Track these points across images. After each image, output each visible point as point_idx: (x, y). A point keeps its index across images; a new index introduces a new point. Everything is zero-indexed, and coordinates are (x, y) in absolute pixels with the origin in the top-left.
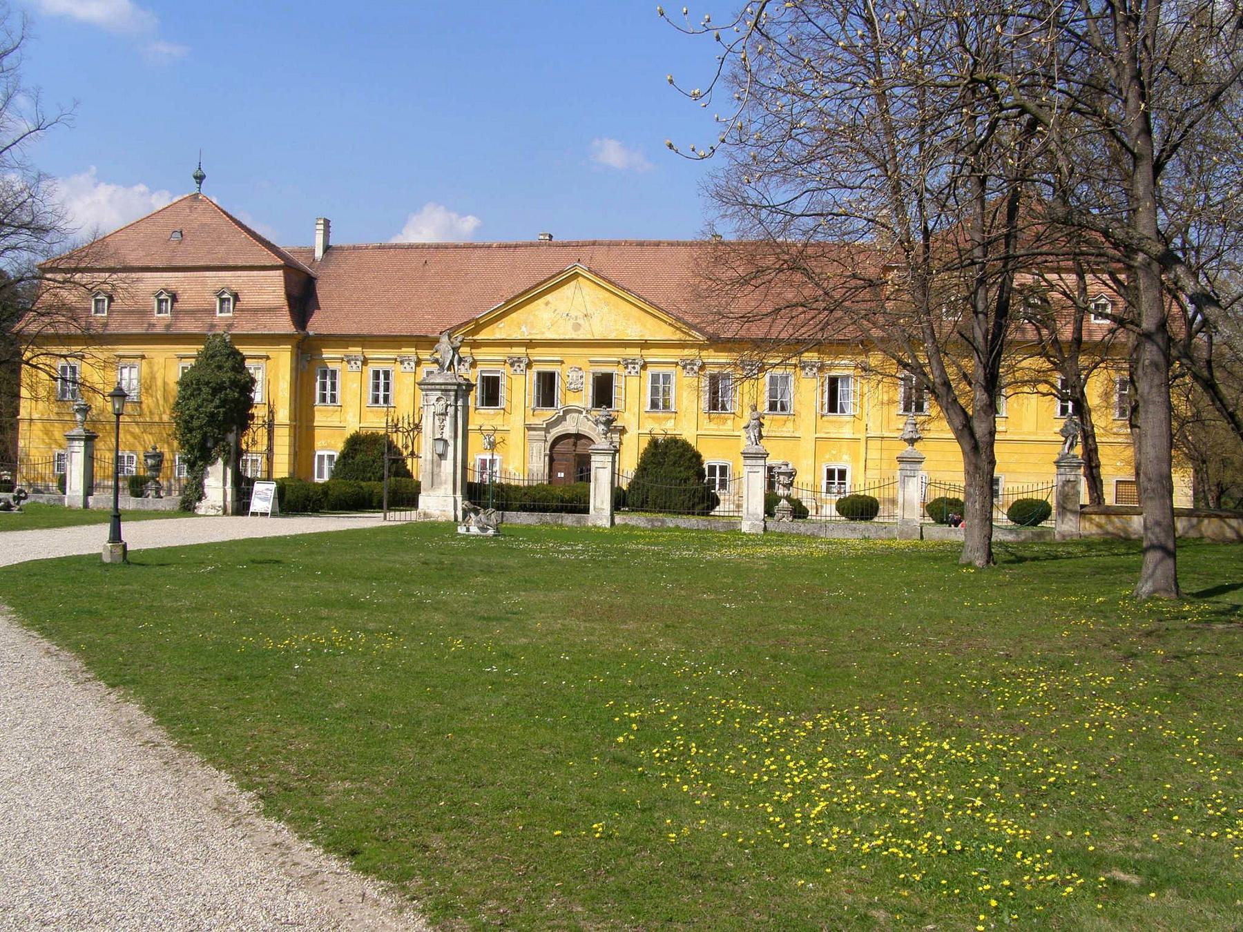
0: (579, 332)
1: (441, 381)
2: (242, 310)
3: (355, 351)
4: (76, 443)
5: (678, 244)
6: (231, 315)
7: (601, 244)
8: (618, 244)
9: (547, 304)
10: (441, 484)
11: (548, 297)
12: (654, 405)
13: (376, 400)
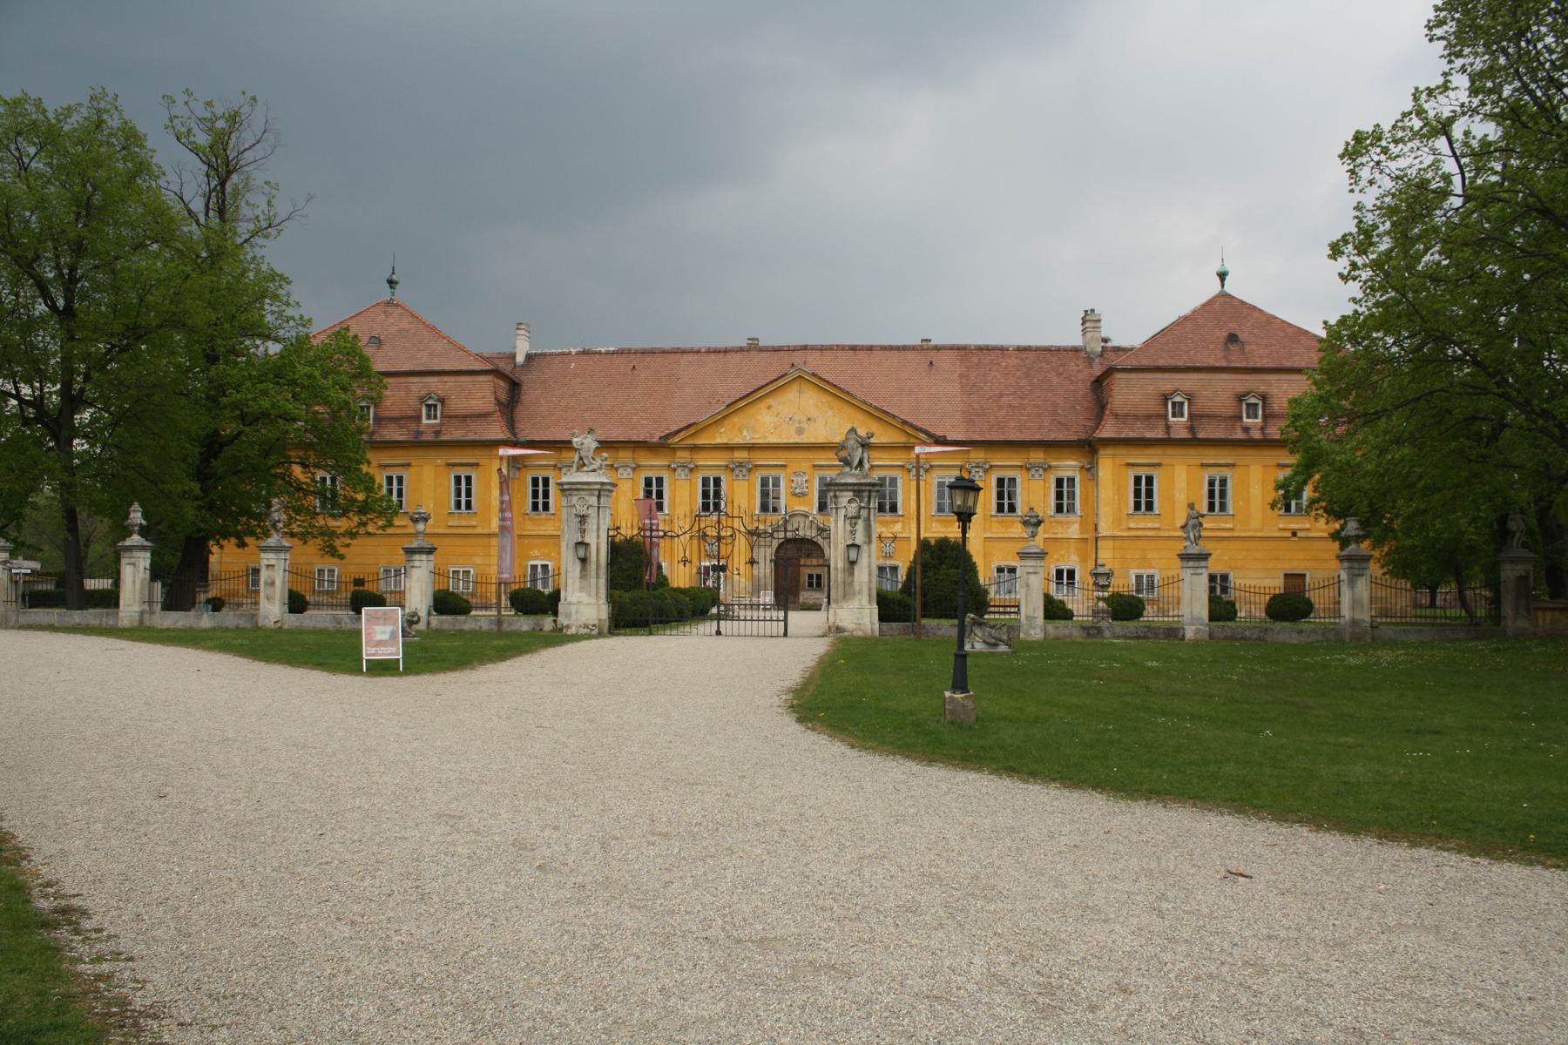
2: (450, 417)
4: (417, 557)
6: (438, 421)
9: (769, 407)
10: (854, 594)
11: (771, 401)
12: (1000, 508)
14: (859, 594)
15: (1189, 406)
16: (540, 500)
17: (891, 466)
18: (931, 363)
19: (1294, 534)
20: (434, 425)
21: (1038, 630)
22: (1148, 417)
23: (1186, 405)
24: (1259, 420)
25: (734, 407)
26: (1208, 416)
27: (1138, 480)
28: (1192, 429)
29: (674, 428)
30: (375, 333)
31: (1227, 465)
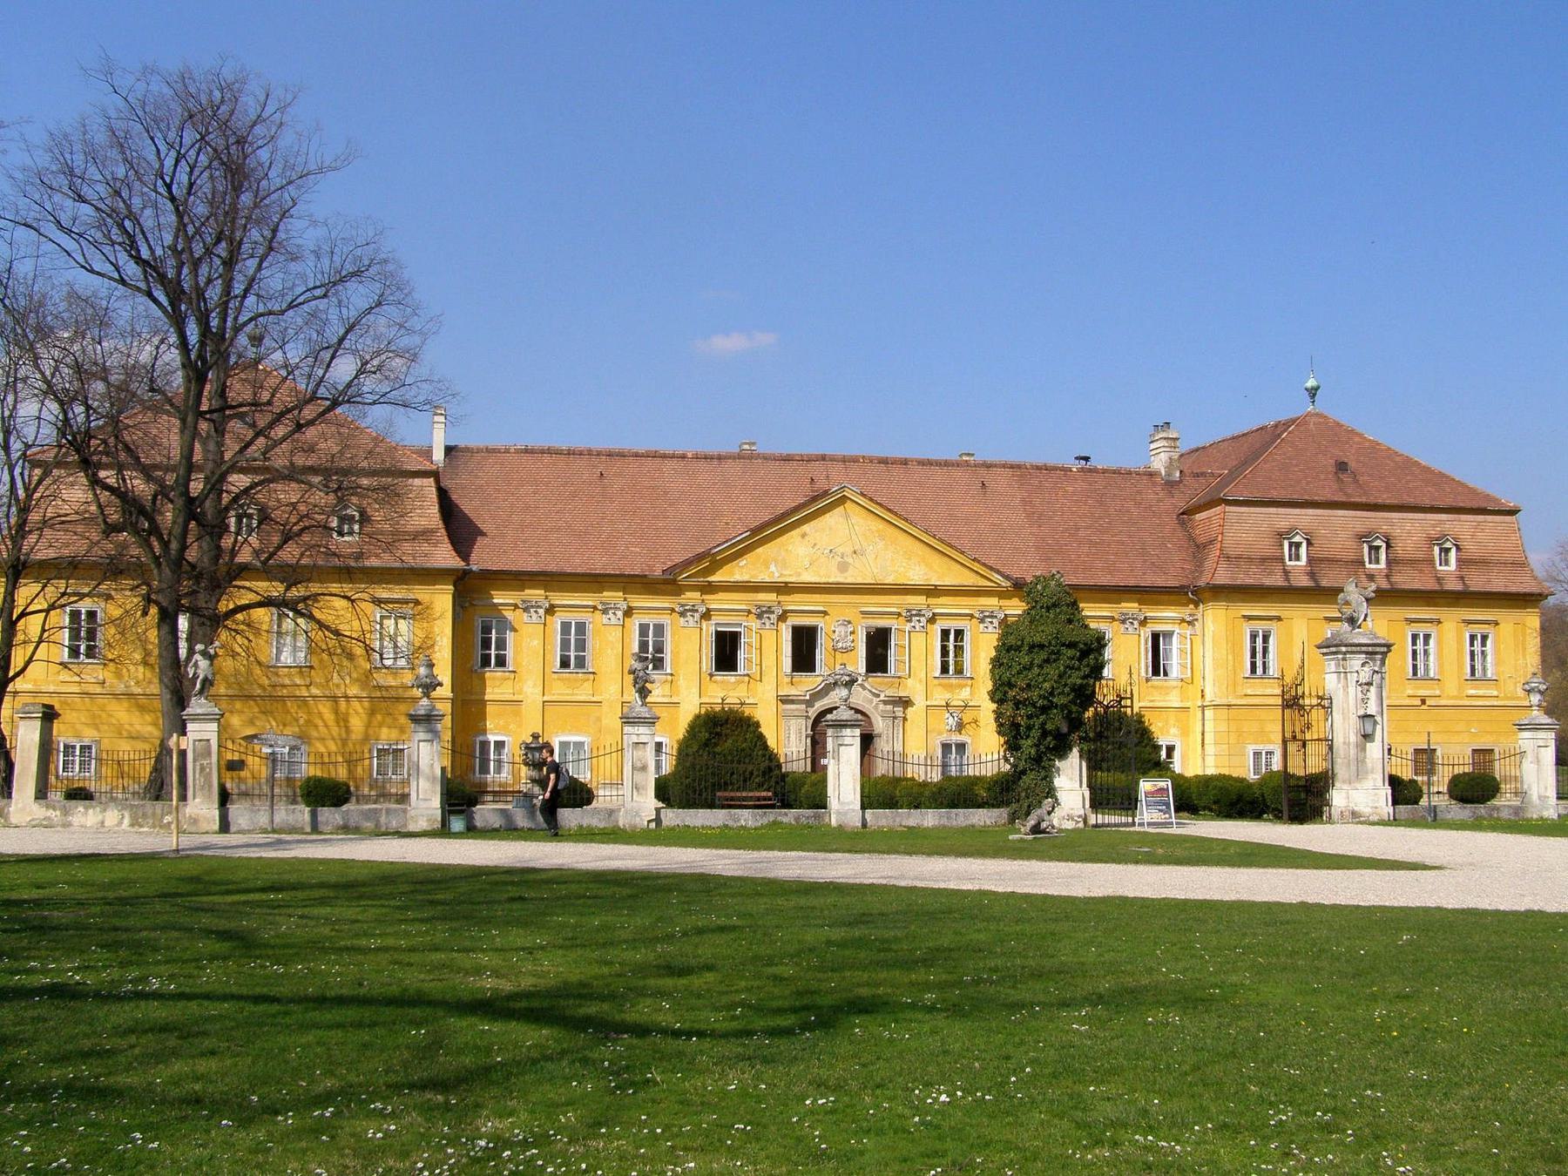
0: (845, 574)
3: (535, 594)
4: (848, 732)
5: (930, 463)
7: (833, 459)
8: (855, 460)
9: (804, 536)
11: (806, 528)
13: (945, 669)
14: (1372, 772)
15: (1387, 549)
17: (956, 615)
19: (1423, 702)
21: (1552, 810)
22: (1263, 560)
23: (1304, 545)
24: (1383, 565)
26: (1328, 560)
28: (1312, 575)
31: (1430, 621)
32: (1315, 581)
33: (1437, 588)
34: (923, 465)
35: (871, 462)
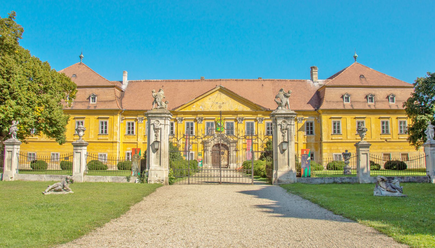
0: (221, 109)
1: (284, 112)
6: (96, 103)
9: (210, 99)
16: (131, 130)
18: (263, 85)
20: (94, 104)
22: (337, 102)
25: (198, 98)
27: (335, 124)
28: (352, 106)
29: (177, 106)
30: (75, 73)
32: (353, 107)
33: (389, 108)
34: (247, 81)
35: (233, 80)
